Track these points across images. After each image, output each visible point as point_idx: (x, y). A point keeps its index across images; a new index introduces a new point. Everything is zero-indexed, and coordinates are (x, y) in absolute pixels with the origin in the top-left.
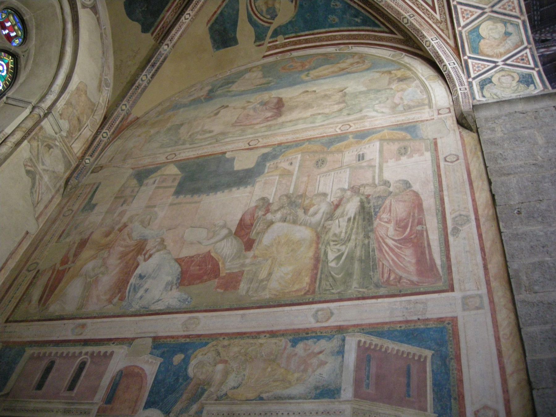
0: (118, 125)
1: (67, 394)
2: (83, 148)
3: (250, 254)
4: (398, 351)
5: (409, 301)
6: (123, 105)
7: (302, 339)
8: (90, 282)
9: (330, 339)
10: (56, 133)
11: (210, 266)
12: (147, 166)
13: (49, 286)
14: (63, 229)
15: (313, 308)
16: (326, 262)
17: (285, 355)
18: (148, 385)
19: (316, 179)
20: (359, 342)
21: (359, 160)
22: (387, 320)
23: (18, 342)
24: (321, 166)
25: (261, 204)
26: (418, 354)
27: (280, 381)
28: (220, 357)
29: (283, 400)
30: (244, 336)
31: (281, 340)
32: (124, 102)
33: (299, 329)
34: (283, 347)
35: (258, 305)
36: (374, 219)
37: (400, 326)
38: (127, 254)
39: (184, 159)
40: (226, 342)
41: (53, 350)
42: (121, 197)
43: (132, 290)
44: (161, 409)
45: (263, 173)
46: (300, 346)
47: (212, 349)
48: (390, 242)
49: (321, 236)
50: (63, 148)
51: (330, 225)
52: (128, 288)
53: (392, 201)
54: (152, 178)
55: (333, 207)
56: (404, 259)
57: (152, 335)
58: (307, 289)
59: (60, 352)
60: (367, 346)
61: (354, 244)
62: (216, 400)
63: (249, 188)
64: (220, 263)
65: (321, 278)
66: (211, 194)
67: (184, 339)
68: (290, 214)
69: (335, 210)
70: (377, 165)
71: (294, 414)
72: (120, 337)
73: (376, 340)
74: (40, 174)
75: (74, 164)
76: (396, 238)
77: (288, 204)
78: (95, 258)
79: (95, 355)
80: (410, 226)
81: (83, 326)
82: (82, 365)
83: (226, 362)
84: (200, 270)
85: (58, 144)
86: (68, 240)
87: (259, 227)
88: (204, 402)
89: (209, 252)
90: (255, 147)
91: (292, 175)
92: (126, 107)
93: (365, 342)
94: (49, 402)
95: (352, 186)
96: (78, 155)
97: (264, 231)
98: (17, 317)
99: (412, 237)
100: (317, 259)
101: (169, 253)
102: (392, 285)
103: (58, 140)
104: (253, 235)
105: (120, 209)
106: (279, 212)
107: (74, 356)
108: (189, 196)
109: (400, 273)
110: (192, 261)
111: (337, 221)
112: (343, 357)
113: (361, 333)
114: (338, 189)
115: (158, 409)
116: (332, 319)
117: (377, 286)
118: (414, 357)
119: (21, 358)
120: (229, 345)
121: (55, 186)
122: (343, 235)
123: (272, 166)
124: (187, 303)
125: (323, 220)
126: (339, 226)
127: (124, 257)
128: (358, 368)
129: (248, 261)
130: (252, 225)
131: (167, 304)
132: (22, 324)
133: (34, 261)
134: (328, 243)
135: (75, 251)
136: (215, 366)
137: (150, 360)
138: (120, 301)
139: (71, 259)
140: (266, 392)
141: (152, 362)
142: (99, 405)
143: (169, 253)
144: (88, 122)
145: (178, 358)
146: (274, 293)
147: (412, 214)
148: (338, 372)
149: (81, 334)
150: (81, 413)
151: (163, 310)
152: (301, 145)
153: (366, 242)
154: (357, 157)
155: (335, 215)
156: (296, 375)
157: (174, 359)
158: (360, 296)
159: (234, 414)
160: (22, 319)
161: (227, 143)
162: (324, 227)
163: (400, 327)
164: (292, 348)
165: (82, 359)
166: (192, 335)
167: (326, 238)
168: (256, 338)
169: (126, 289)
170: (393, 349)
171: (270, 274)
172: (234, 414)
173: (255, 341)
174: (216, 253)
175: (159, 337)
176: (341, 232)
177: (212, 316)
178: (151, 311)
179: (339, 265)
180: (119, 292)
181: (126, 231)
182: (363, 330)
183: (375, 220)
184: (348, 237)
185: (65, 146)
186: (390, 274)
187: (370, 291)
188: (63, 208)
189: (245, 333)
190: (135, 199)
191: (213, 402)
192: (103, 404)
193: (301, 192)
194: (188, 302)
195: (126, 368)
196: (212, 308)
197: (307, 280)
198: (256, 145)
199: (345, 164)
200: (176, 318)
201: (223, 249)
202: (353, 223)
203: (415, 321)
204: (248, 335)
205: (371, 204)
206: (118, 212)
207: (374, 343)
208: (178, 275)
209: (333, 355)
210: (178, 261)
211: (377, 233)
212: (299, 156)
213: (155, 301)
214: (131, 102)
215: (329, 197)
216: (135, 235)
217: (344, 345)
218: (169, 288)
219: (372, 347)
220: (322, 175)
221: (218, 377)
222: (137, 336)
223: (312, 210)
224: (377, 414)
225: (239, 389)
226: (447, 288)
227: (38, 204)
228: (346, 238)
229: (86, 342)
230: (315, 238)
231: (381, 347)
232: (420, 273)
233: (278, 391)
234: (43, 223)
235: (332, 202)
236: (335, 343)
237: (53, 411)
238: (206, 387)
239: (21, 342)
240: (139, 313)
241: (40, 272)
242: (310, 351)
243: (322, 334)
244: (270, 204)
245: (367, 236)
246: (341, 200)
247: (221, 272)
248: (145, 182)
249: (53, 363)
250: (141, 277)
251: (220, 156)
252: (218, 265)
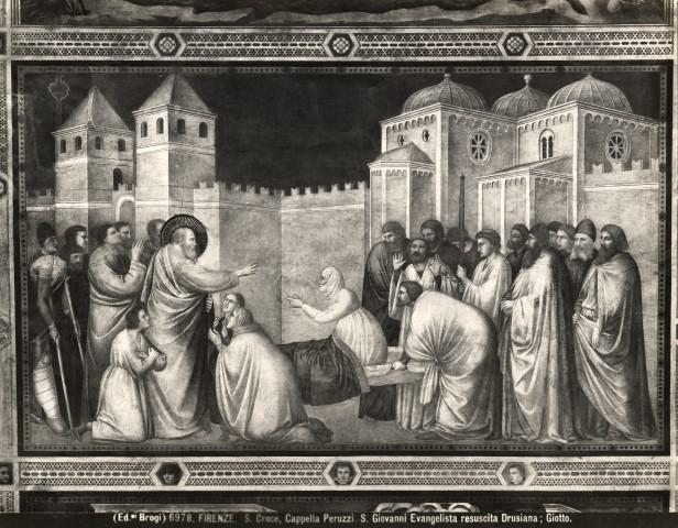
114: (514, 228)
226: (663, 449)
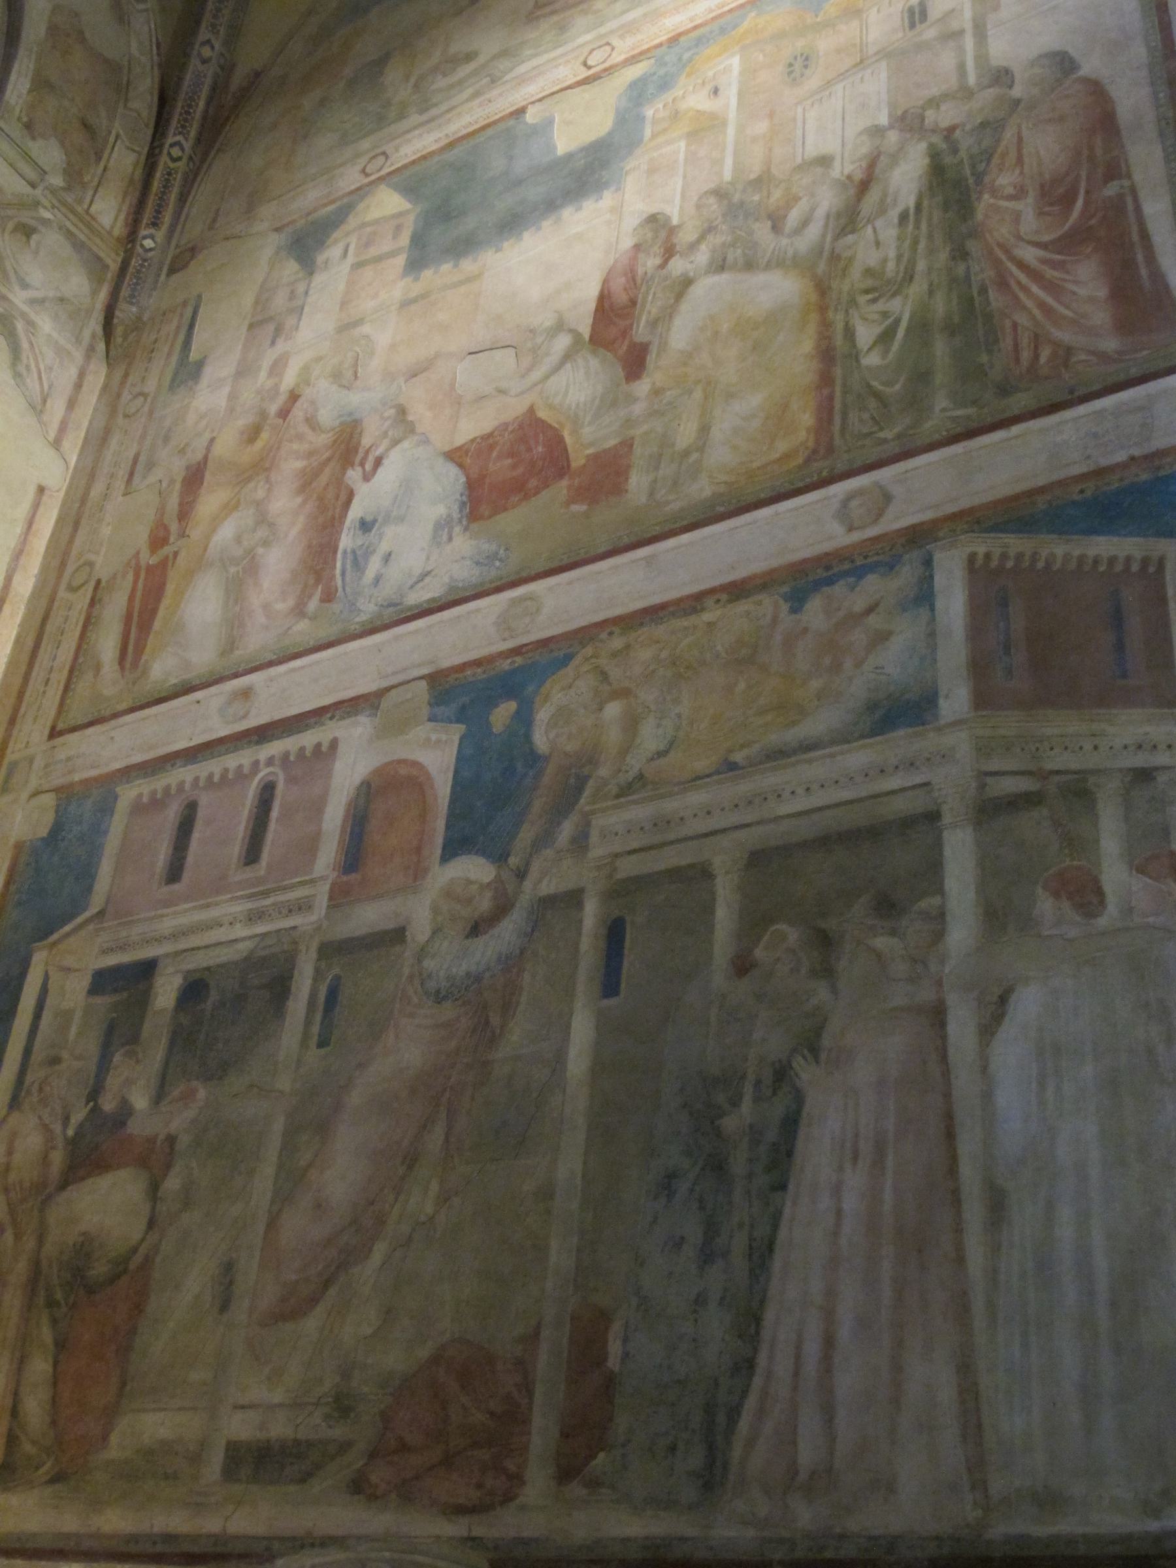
0: (206, 111)
1: (249, 873)
2: (125, 208)
3: (642, 387)
4: (1081, 559)
5: (1100, 413)
6: (203, 44)
7: (817, 585)
8: (238, 572)
9: (892, 568)
10: (33, 186)
11: (540, 449)
12: (315, 210)
13: (136, 615)
14: (131, 454)
15: (835, 496)
16: (854, 355)
17: (778, 638)
18: (440, 800)
19: (794, 120)
20: (972, 558)
21: (912, 25)
22: (1041, 481)
23: (96, 779)
24: (802, 75)
25: (650, 235)
26: (1138, 554)
28: (610, 684)
29: (789, 756)
30: (661, 614)
31: (760, 603)
32: (204, 34)
33: (805, 561)
35: (685, 523)
36: (974, 196)
37: (1080, 488)
38: (316, 473)
39: (413, 162)
40: (617, 643)
41: (184, 774)
42: (262, 322)
43: (348, 566)
44: (483, 852)
45: (641, 141)
46: (815, 604)
47: (585, 668)
48: (1029, 254)
49: (830, 288)
50: (68, 224)
51: (849, 247)
52: (339, 565)
53: (1023, 127)
54: (336, 241)
55: (852, 192)
56: (1074, 293)
57: (425, 671)
58: (811, 444)
59: (204, 775)
60: (994, 563)
61: (925, 287)
62: (617, 796)
63: (608, 198)
64: (566, 434)
65: (845, 405)
66: (506, 244)
67: (509, 661)
68: (733, 245)
69: (859, 200)
70: (968, 26)
71: (822, 786)
72: (346, 698)
73: (1016, 544)
74: (24, 315)
75: (114, 261)
76: (1047, 238)
77: (724, 215)
78: (236, 507)
79: (292, 758)
80: (1082, 192)
81: (246, 694)
82: (267, 793)
83: (623, 693)
84: (514, 467)
85: (47, 215)
86: (152, 479)
87: (651, 307)
88: (587, 808)
89: (531, 410)
90: (605, 70)
91: (724, 123)
92: (213, 48)
93: (988, 556)
94: (208, 906)
95: (899, 113)
96: (117, 232)
97: (668, 313)
98: (76, 715)
99: (1093, 222)
100: (826, 355)
101: (426, 441)
102: (1046, 378)
103: (47, 203)
104: (641, 332)
105: (270, 356)
106: (703, 247)
107: (242, 776)
108: (446, 267)
109: (1064, 336)
110: (491, 448)
111: (869, 230)
112: (932, 609)
113: (973, 531)
114: (861, 134)
115: (476, 853)
116: (892, 511)
117: (1004, 390)
118: (1127, 568)
119: (112, 815)
120: (628, 647)
121: (78, 340)
122: (891, 265)
123: (661, 114)
124: (497, 563)
125: (829, 239)
126: (878, 244)
127: (311, 483)
128: (975, 632)
129: (638, 409)
130: (633, 302)
131: (446, 579)
132: (91, 730)
133: (82, 561)
134: (853, 302)
135: (181, 504)
136: (601, 710)
137: (434, 737)
138: (327, 605)
139: (174, 527)
140: (742, 746)
141: (439, 741)
142: (330, 881)
143: (426, 441)
144: (117, 127)
145: (502, 714)
146: (724, 478)
147: (1085, 152)
149: (244, 717)
150: (290, 911)
151: (440, 597)
152: (735, 26)
153: (961, 269)
154: (906, 15)
155: (862, 214)
156: (815, 684)
157: (492, 718)
158: (959, 430)
159: (668, 822)
160: (90, 718)
161: (523, 80)
162: (834, 257)
163: (1082, 491)
164: (793, 617)
165: (262, 779)
166: (526, 645)
167: (846, 288)
168: (695, 611)
169: (334, 567)
170: (1067, 557)
171: (705, 429)
172: (668, 822)
173: (693, 620)
174: (551, 407)
175: (442, 671)
176: (885, 261)
177: (570, 583)
178: (410, 608)
179: (891, 356)
180: (318, 580)
181: (298, 412)
182: (978, 522)
183: (979, 199)
184: (906, 268)
185: (71, 216)
186: (1036, 347)
187: (986, 410)
188: (119, 396)
189: (663, 607)
190: (304, 317)
191: (610, 803)
192: (338, 876)
193: (755, 171)
194: (501, 560)
195: (378, 772)
196: (566, 561)
197: (807, 419)
198: (604, 62)
199: (871, 52)
200: (478, 610)
201: (567, 392)
202: (917, 226)
203: (1123, 466)
204: (671, 609)
205: (963, 154)
206: (266, 364)
207: (1012, 553)
208: (462, 495)
209: (904, 610)
210: (455, 456)
211: (987, 235)
212: (735, 62)
213: (414, 579)
214: (222, 31)
215: (837, 164)
216: (327, 416)
217: (931, 577)
218: (445, 538)
219: (1010, 564)
220: (809, 102)
221: (614, 736)
222: (385, 684)
223: (794, 217)
224: (1041, 741)
227: (44, 401)
228: (901, 275)
229: (263, 734)
230: (814, 297)
231: (1034, 557)
232: (1124, 326)
234: (77, 451)
235: (849, 177)
236: (907, 575)
237: (221, 926)
238: (586, 771)
239: (101, 776)
240: (379, 623)
241: (103, 584)
243: (869, 560)
244: (672, 231)
245: (960, 254)
246: (872, 164)
247: (572, 455)
248: (320, 259)
249: (191, 809)
250: (365, 526)
251: (512, 122)
252: (560, 440)
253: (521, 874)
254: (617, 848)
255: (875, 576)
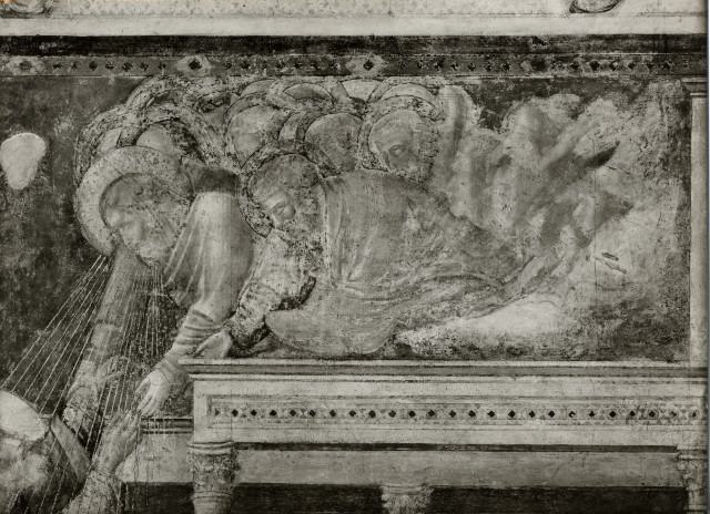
17: (463, 162)
27: (460, 277)
28: (201, 158)
29: (484, 358)
31: (435, 91)
34: (450, 122)
47: (156, 115)
67: (18, 60)
120: (226, 100)
136: (192, 199)
140: (417, 325)
148: (674, 249)
159: (312, 413)
164: (487, 132)
173: (329, 84)
225: (311, 305)
233: (461, 322)
238: (177, 297)
242: (560, 150)
253: (89, 441)
254: (239, 437)
255: (609, 103)
